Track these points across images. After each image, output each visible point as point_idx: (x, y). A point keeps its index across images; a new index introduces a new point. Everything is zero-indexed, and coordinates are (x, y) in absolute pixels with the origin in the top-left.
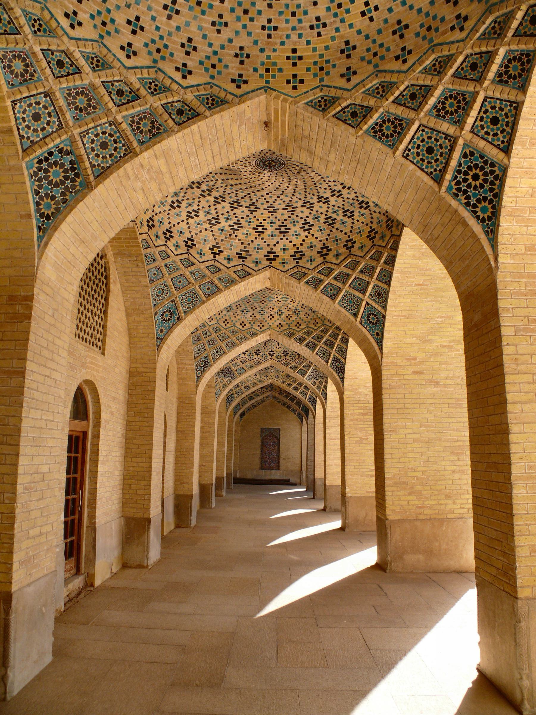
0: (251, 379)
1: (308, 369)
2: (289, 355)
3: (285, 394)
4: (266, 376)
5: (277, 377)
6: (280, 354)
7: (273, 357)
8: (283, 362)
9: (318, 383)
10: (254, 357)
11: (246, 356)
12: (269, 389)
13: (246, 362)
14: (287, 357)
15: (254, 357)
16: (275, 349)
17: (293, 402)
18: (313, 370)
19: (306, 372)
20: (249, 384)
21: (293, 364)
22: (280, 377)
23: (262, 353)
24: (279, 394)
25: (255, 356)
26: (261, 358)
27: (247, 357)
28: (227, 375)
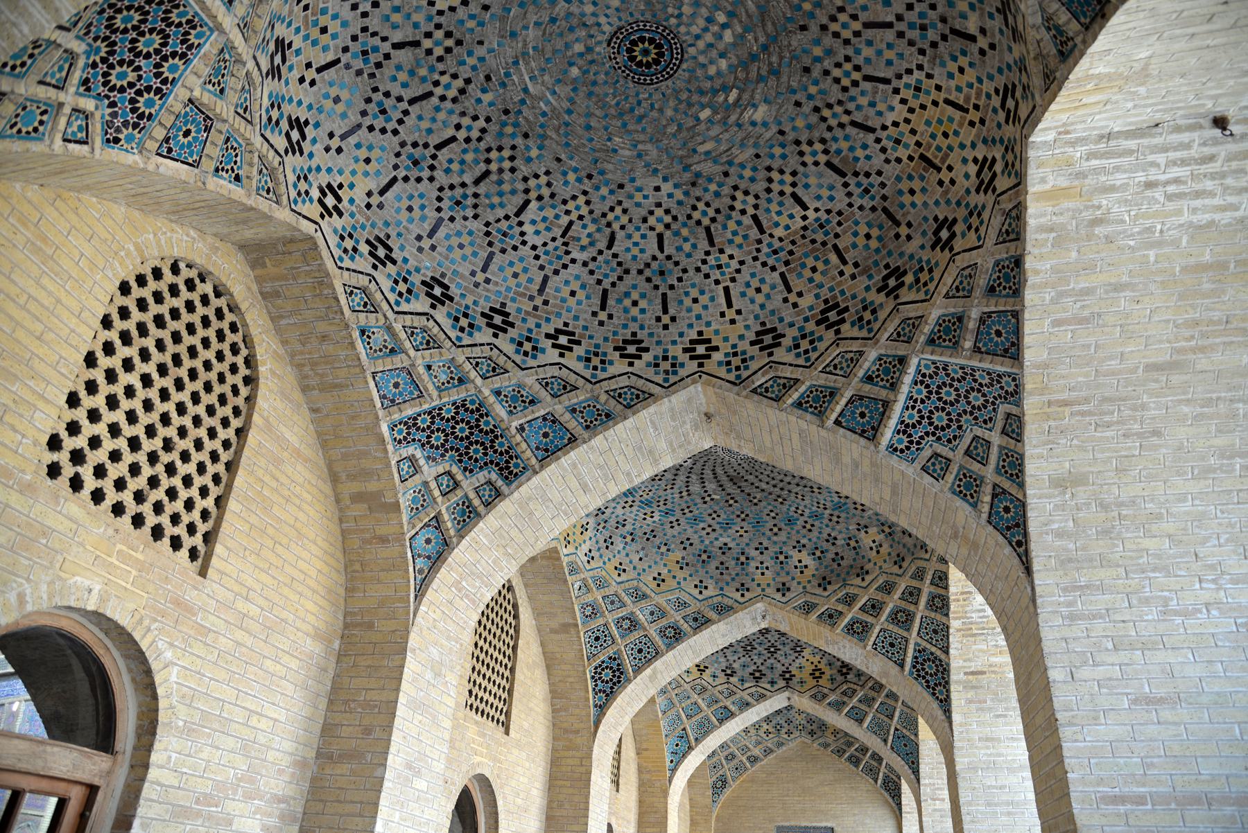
0: (687, 598)
1: (893, 387)
2: (787, 342)
3: (832, 698)
4: (743, 588)
5: (783, 589)
6: (744, 346)
7: (710, 366)
8: (759, 380)
9: (958, 457)
10: (612, 370)
11: (570, 360)
12: (782, 683)
13: (568, 388)
14: (780, 354)
15: (612, 370)
16: (717, 328)
17: (860, 721)
18: (921, 379)
19: (887, 404)
20: (676, 617)
21: (813, 379)
22: (796, 589)
23: (657, 351)
24: (814, 697)
25: (620, 366)
26: (650, 373)
27: (579, 367)
28: (476, 451)
